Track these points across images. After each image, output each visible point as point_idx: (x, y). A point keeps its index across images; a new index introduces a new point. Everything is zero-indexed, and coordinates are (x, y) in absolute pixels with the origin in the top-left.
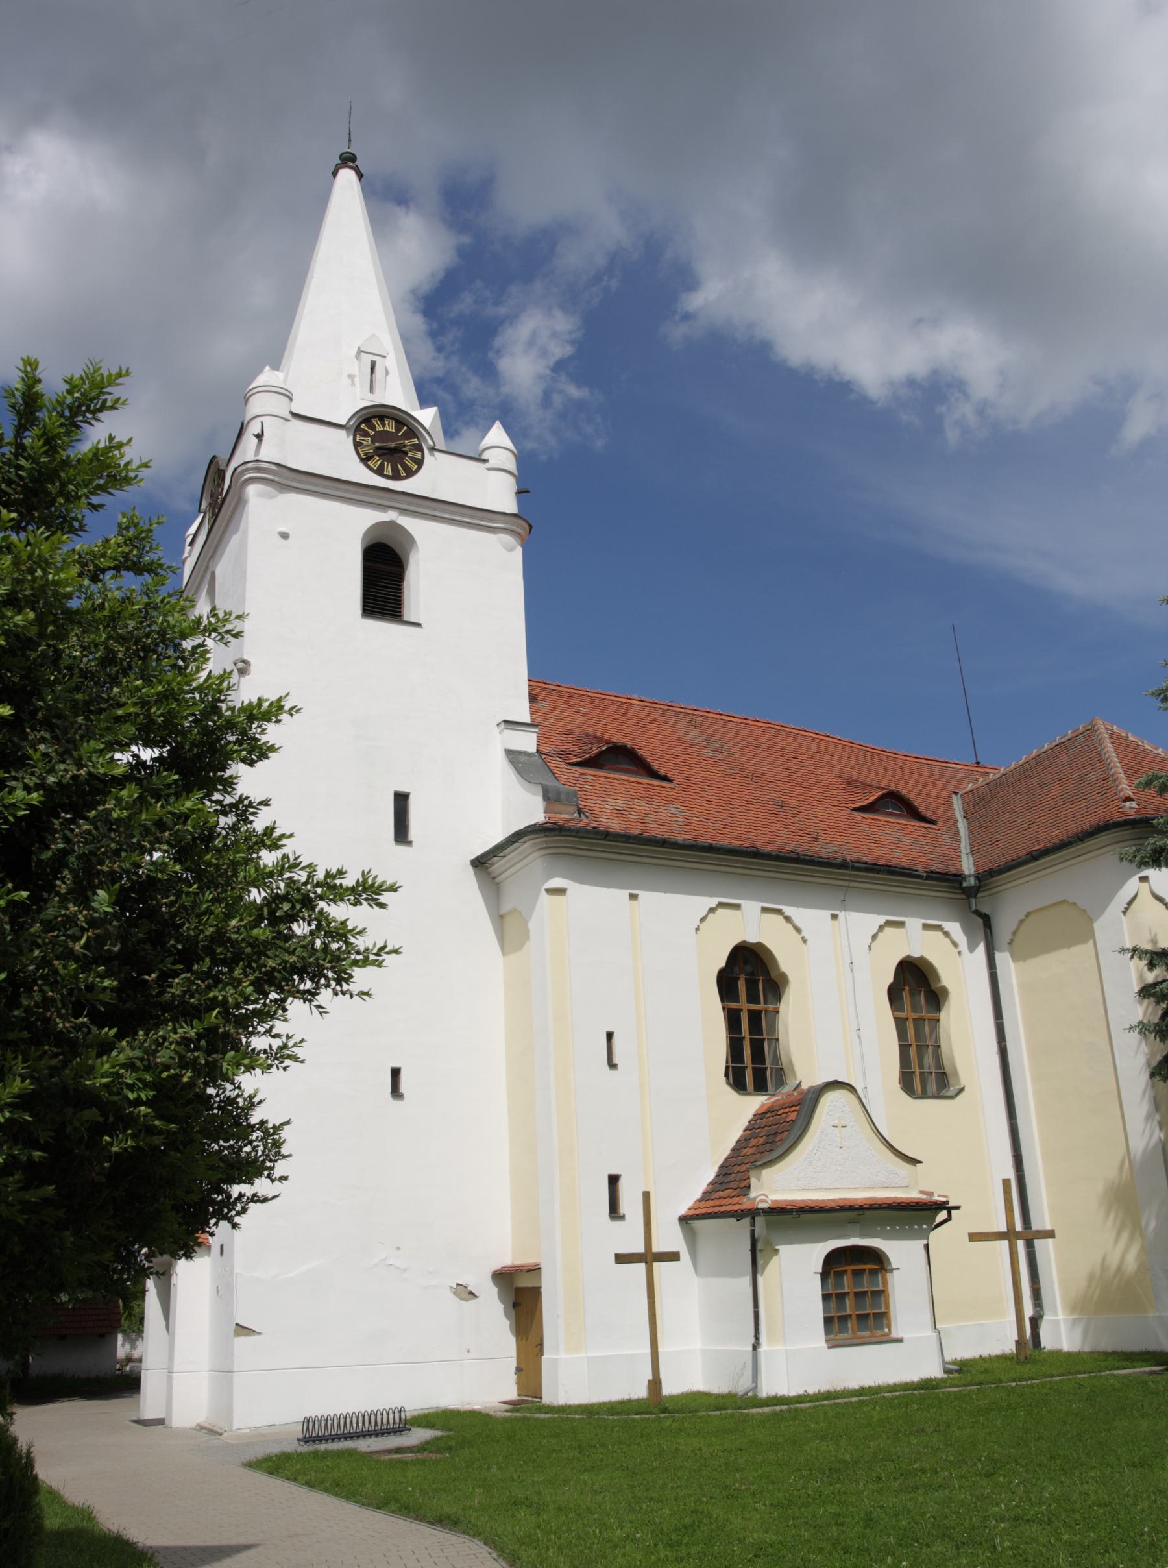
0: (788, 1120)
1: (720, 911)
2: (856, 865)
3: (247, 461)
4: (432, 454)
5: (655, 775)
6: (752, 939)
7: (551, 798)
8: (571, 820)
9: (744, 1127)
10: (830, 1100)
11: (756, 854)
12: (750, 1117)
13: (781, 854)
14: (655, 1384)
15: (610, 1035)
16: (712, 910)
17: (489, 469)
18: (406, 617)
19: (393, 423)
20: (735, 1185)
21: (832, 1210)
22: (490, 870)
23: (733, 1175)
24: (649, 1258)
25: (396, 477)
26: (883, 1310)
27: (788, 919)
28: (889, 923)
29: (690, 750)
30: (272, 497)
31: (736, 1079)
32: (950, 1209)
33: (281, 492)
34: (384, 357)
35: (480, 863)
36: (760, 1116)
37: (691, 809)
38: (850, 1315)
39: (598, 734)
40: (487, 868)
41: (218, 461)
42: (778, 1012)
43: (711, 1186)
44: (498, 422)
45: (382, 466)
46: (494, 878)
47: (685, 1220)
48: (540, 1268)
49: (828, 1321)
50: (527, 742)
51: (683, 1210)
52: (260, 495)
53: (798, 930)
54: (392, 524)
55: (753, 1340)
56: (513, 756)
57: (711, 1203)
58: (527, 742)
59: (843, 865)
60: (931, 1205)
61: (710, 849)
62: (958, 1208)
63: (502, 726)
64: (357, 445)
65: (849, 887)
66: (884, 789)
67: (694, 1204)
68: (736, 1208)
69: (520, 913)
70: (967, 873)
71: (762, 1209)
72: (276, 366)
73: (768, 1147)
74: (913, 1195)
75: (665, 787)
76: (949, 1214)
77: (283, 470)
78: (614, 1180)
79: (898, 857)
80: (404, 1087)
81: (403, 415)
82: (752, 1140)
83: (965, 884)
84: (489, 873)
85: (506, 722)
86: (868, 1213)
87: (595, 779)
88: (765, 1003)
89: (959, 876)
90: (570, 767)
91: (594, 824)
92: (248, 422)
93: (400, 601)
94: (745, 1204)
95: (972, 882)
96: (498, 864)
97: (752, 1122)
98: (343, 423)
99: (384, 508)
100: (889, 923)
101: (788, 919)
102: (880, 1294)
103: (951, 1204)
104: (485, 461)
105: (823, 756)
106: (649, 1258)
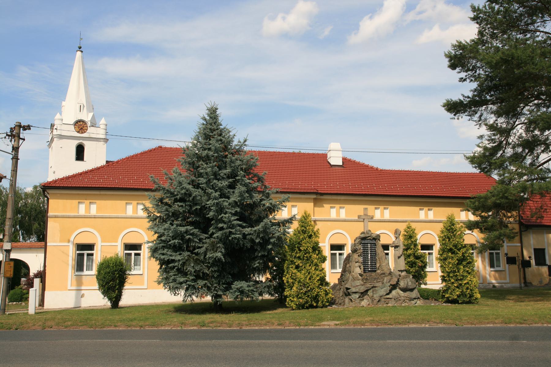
25: (82, 133)
33: (60, 139)
54: (81, 142)
64: (75, 128)
104: (100, 127)
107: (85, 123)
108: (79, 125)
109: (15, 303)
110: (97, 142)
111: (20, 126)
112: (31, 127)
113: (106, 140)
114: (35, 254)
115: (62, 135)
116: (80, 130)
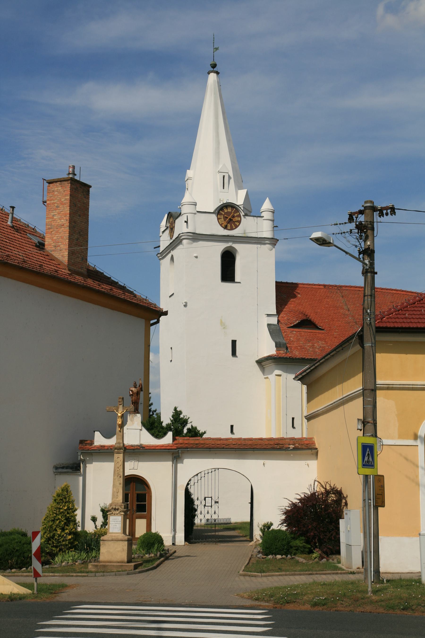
3: (183, 232)
4: (245, 218)
7: (278, 346)
15: (293, 419)
17: (263, 220)
18: (236, 281)
19: (230, 209)
25: (232, 229)
30: (192, 244)
34: (228, 173)
37: (326, 343)
41: (171, 214)
46: (263, 366)
50: (274, 321)
52: (188, 243)
54: (231, 247)
56: (269, 325)
58: (274, 321)
63: (266, 316)
64: (218, 219)
77: (195, 235)
80: (234, 431)
81: (234, 205)
84: (261, 364)
85: (267, 315)
93: (234, 268)
96: (263, 363)
99: (227, 242)
104: (263, 217)
107: (236, 209)
108: (226, 213)
109: (279, 557)
110: (259, 246)
111: (374, 209)
112: (396, 210)
113: (273, 241)
114: (262, 462)
115: (197, 232)
116: (228, 223)
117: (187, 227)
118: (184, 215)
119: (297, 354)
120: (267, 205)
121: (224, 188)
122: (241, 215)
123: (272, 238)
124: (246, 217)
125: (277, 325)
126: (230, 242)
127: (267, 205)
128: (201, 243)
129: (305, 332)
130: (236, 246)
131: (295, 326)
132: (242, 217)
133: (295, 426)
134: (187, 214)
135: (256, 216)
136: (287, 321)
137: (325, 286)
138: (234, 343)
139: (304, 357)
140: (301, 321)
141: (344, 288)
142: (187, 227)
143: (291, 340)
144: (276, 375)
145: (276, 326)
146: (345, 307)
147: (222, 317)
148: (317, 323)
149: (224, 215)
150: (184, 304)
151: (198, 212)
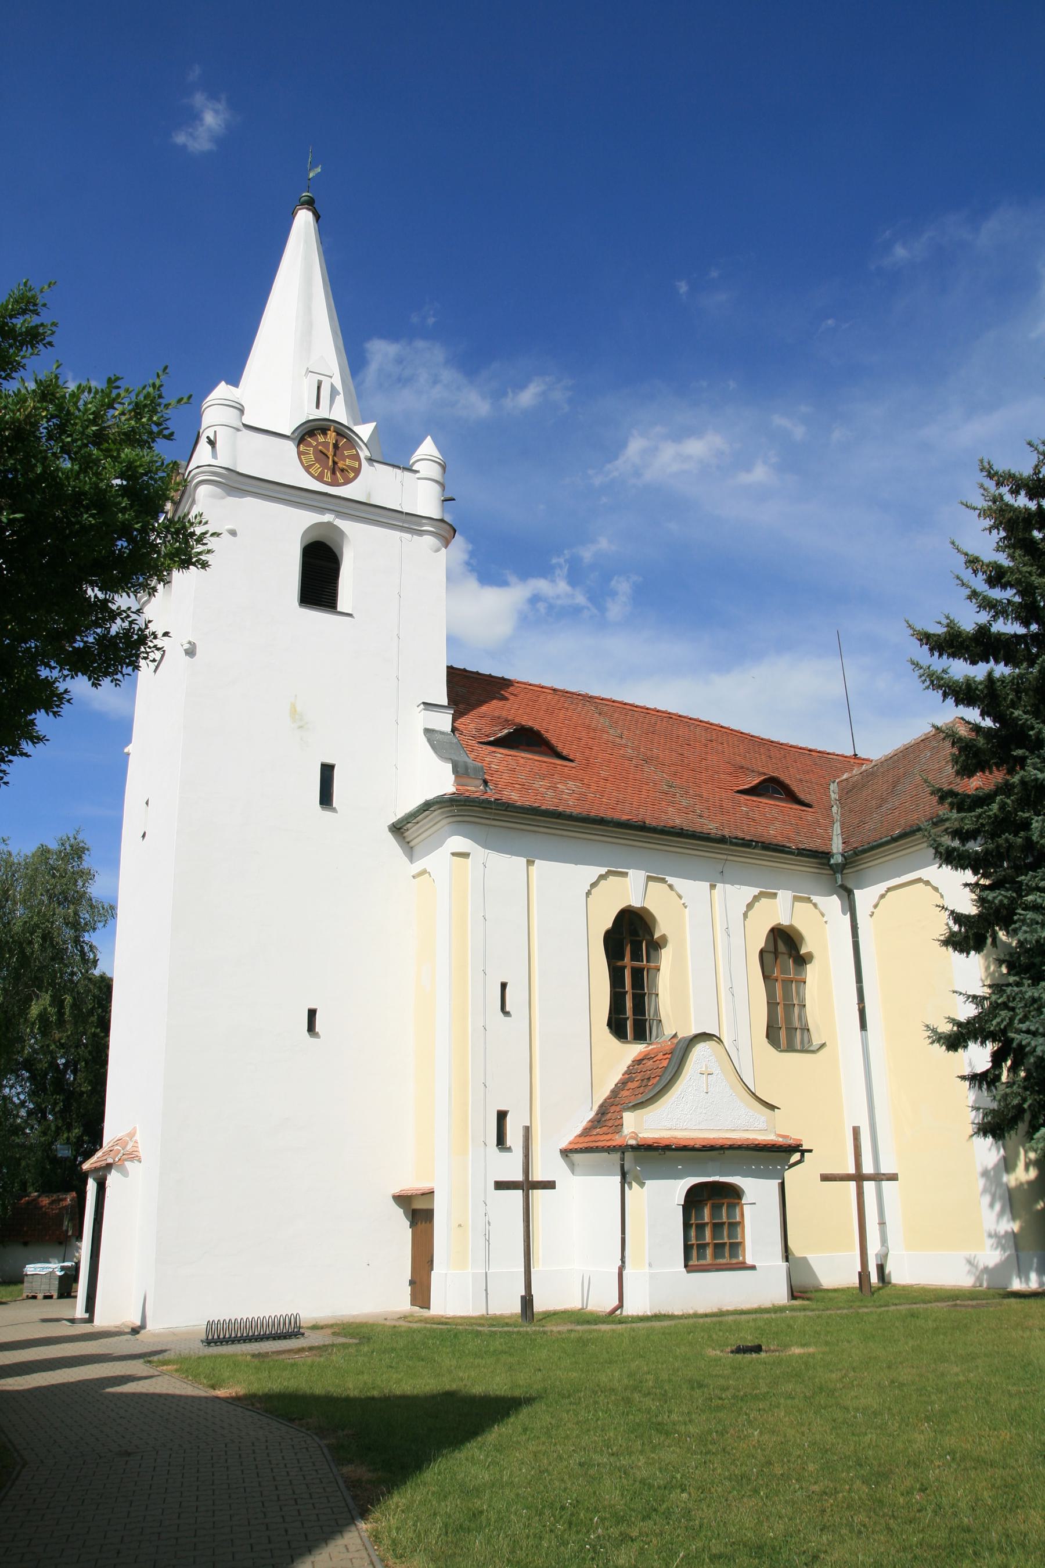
0: (660, 1066)
1: (611, 878)
2: (734, 840)
5: (559, 756)
6: (636, 903)
7: (460, 772)
8: (477, 792)
9: (623, 1072)
10: (700, 1050)
11: (642, 828)
12: (629, 1062)
13: (666, 829)
14: (527, 1301)
15: (504, 986)
16: (602, 877)
17: (418, 479)
18: (339, 609)
20: (610, 1124)
21: (693, 1149)
22: (406, 834)
23: (610, 1114)
24: (528, 1185)
25: (334, 483)
26: (739, 1240)
27: (671, 887)
28: (762, 895)
29: (592, 735)
30: (223, 498)
31: (617, 1026)
32: (803, 1152)
33: (229, 495)
34: (331, 377)
35: (398, 829)
36: (638, 1062)
38: (709, 1244)
39: (510, 718)
40: (403, 833)
42: (659, 970)
43: (590, 1124)
44: (429, 437)
45: (322, 473)
46: (408, 843)
47: (565, 1153)
48: (433, 1192)
49: (687, 1248)
50: (443, 721)
51: (564, 1144)
52: (213, 496)
53: (680, 897)
54: (329, 524)
55: (620, 1263)
57: (587, 1139)
59: (722, 840)
60: (786, 1147)
61: (601, 821)
62: (810, 1151)
63: (422, 706)
64: (300, 454)
65: (726, 860)
66: (765, 774)
67: (574, 1139)
68: (608, 1144)
69: (429, 873)
70: (835, 851)
71: (630, 1145)
72: (234, 381)
73: (641, 1090)
74: (768, 1137)
75: (566, 766)
76: (802, 1156)
77: (234, 476)
78: (502, 1116)
79: (773, 833)
80: (318, 1028)
82: (629, 1083)
83: (832, 861)
84: (404, 838)
86: (727, 1152)
87: (503, 756)
88: (648, 961)
89: (828, 853)
90: (481, 746)
91: (497, 796)
92: (203, 433)
93: (335, 593)
94: (617, 1140)
95: (837, 859)
96: (411, 832)
97: (631, 1068)
98: (289, 434)
99: (322, 510)
100: (762, 895)
101: (671, 887)
102: (735, 1226)
103: (804, 1147)
105: (714, 744)
106: (528, 1185)
107: (349, 440)
108: (319, 444)
110: (408, 536)
117: (214, 455)
118: (206, 431)
119: (514, 796)
120: (428, 448)
121: (318, 406)
122: (362, 456)
123: (442, 520)
124: (375, 464)
125: (450, 735)
126: (327, 511)
127: (428, 448)
128: (250, 502)
129: (525, 760)
130: (343, 524)
131: (499, 743)
132: (364, 463)
133: (508, 1009)
134: (215, 428)
135: (398, 467)
136: (476, 732)
137: (554, 690)
138: (327, 772)
139: (536, 805)
140: (514, 729)
141: (597, 700)
142: (214, 455)
143: (492, 769)
144: (453, 854)
145: (449, 737)
146: (611, 731)
147: (296, 696)
148: (554, 741)
149: (315, 447)
150: (187, 646)
151: (245, 426)
